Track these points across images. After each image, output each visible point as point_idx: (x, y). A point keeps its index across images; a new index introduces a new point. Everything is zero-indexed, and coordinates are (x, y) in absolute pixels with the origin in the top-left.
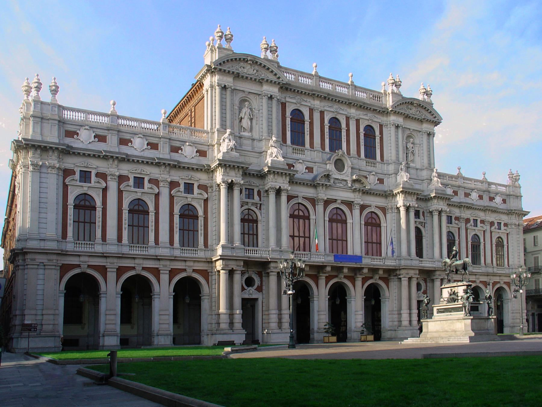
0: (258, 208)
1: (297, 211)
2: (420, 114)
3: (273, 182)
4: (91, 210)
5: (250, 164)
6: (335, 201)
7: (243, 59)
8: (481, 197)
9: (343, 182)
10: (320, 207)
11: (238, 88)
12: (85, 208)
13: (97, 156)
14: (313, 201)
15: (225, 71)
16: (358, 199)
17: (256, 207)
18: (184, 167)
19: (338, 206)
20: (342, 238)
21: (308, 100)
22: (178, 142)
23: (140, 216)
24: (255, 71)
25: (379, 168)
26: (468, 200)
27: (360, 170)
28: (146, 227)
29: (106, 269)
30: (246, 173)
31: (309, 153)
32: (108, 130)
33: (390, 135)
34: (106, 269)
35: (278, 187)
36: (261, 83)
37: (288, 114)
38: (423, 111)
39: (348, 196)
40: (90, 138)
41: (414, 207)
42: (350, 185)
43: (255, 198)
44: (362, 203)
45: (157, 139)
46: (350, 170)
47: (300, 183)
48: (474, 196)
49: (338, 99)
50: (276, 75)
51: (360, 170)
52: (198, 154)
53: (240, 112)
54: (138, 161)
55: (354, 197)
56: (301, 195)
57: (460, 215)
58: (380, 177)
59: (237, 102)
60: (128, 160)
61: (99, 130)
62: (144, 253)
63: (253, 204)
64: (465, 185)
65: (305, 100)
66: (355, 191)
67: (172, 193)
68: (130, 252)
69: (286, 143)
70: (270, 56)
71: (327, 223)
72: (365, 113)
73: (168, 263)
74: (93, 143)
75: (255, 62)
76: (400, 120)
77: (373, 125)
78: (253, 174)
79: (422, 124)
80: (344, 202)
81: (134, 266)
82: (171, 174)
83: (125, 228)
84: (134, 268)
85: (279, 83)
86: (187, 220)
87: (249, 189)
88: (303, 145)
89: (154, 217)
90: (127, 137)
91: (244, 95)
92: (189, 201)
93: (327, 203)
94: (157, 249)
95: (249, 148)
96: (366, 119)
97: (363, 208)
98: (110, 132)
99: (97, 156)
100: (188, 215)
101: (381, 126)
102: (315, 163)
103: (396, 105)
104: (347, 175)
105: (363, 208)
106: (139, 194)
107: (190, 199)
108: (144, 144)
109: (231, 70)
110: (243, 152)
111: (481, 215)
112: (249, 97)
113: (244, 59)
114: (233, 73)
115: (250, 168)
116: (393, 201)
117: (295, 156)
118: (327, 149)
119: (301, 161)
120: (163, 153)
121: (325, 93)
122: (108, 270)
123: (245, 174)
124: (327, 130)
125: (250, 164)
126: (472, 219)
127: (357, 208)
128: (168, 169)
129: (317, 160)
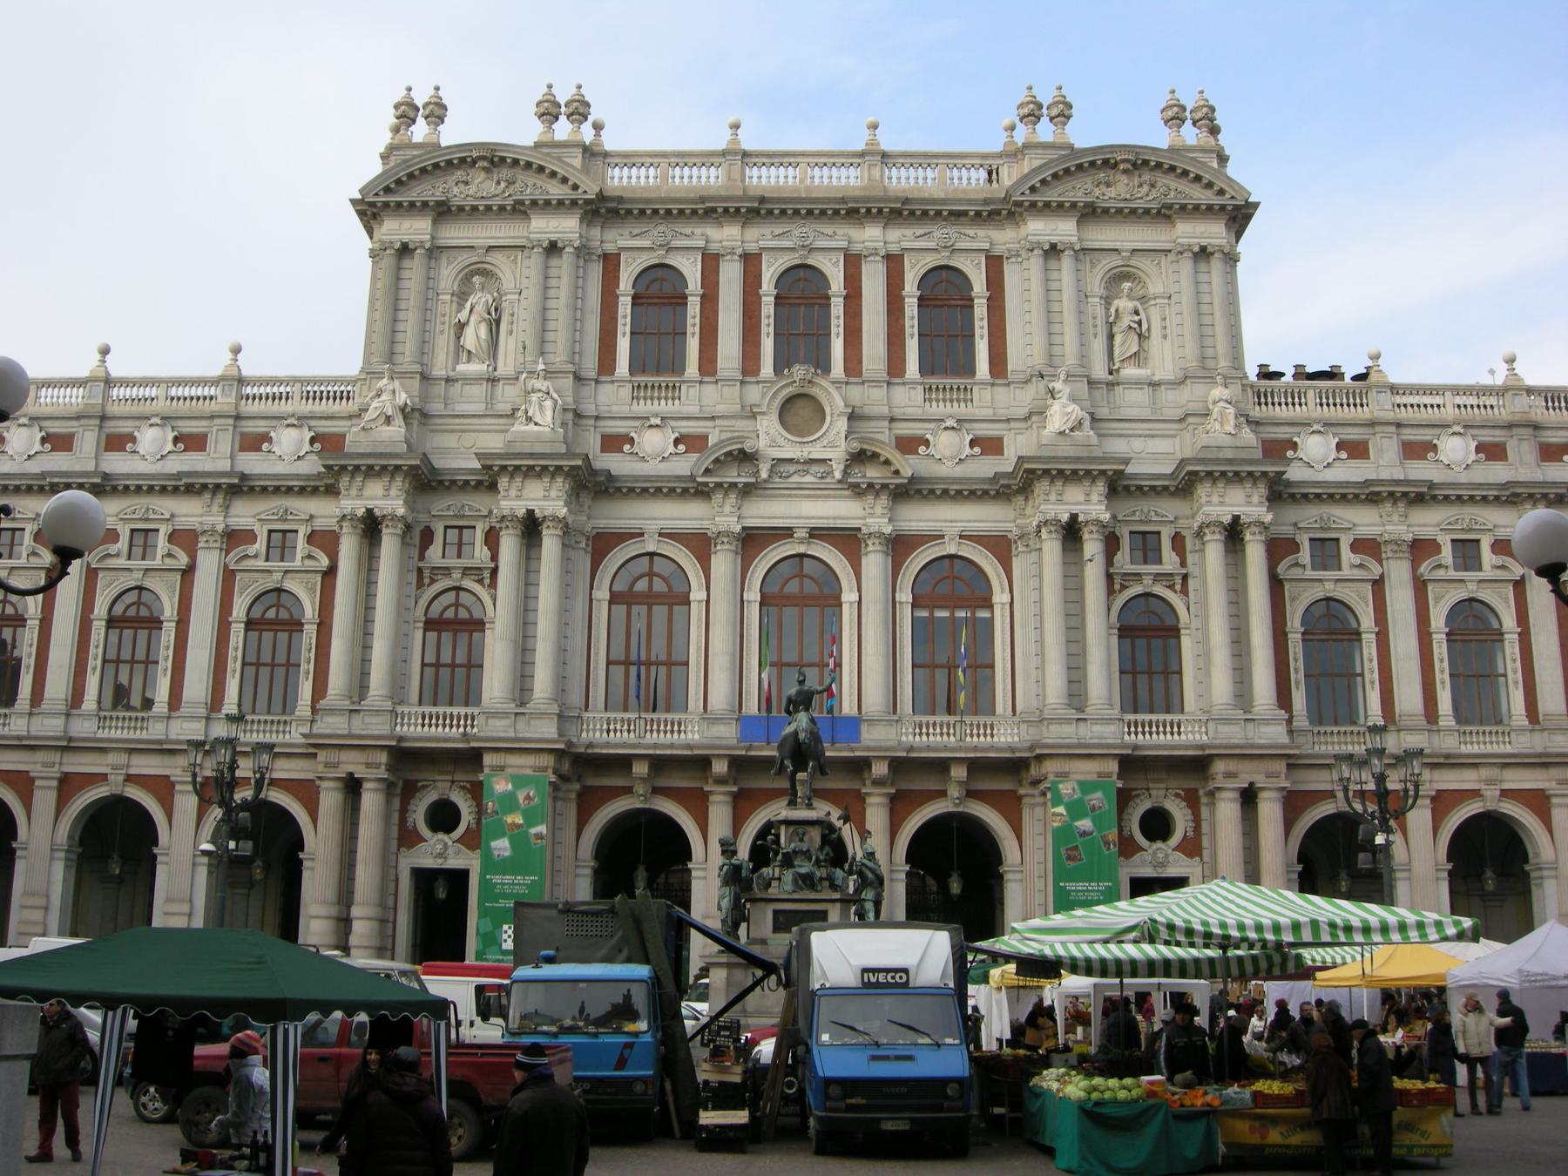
0: (1178, 587)
1: (796, 582)
2: (1183, 196)
3: (1221, 503)
4: (151, 629)
5: (1127, 462)
6: (786, 533)
7: (1105, 162)
8: (1492, 452)
9: (815, 468)
10: (723, 562)
11: (1097, 245)
12: (276, 625)
13: (188, 487)
14: (701, 545)
15: (1047, 205)
16: (872, 517)
17: (480, 581)
18: (264, 489)
19: (802, 549)
20: (669, 654)
21: (698, 231)
22: (262, 423)
23: (1139, 642)
24: (1146, 188)
25: (987, 401)
26: (1421, 471)
27: (892, 420)
28: (291, 666)
29: (173, 784)
30: (1118, 486)
31: (987, 393)
32: (78, 418)
33: (1021, 282)
34: (173, 784)
35: (1065, 517)
36: (1168, 217)
37: (911, 288)
38: (1164, 181)
39: (842, 511)
40: (32, 446)
41: (1098, 522)
42: (838, 475)
43: (477, 554)
44: (888, 530)
45: (204, 423)
46: (842, 425)
47: (645, 490)
48: (1455, 450)
49: (804, 207)
50: (1210, 185)
51: (892, 420)
52: (1344, 455)
53: (461, 306)
54: (139, 488)
55: (861, 513)
56: (652, 527)
57: (1377, 530)
58: (684, 431)
59: (1096, 285)
60: (114, 488)
61: (57, 423)
62: (138, 735)
63: (1157, 577)
64: (1403, 414)
65: (688, 231)
66: (858, 491)
67: (1280, 569)
68: (100, 734)
69: (756, 372)
70: (1190, 135)
71: (753, 612)
72: (919, 232)
73: (55, 757)
74: (172, 457)
75: (1140, 162)
76: (1064, 230)
77: (959, 262)
78: (467, 482)
79: (1173, 224)
80: (816, 534)
81: (311, 776)
82: (232, 511)
83: (94, 669)
84: (103, 777)
85: (1223, 208)
86: (286, 635)
87: (1144, 533)
88: (677, 366)
89: (37, 631)
90: (124, 427)
91: (1120, 262)
92: (1330, 589)
93: (751, 541)
94: (521, 724)
95: (479, 408)
96: (921, 248)
97: (900, 546)
98: (1013, 425)
99: (188, 487)
100: (273, 620)
101: (995, 265)
102: (713, 418)
103: (1035, 181)
104: (832, 443)
105: (900, 546)
106: (1148, 581)
107: (1327, 585)
108: (165, 440)
109: (1068, 198)
110: (457, 421)
111: (1366, 521)
112: (1132, 262)
113: (1106, 162)
114: (1074, 205)
115: (1130, 470)
116: (1029, 511)
117: (641, 408)
118: (767, 369)
119: (655, 421)
120: (216, 459)
121: (896, 200)
122: (37, 783)
123: (1183, 490)
124: (768, 307)
125: (1127, 462)
126: (1445, 541)
127: (870, 548)
128: (220, 498)
129: (721, 409)
